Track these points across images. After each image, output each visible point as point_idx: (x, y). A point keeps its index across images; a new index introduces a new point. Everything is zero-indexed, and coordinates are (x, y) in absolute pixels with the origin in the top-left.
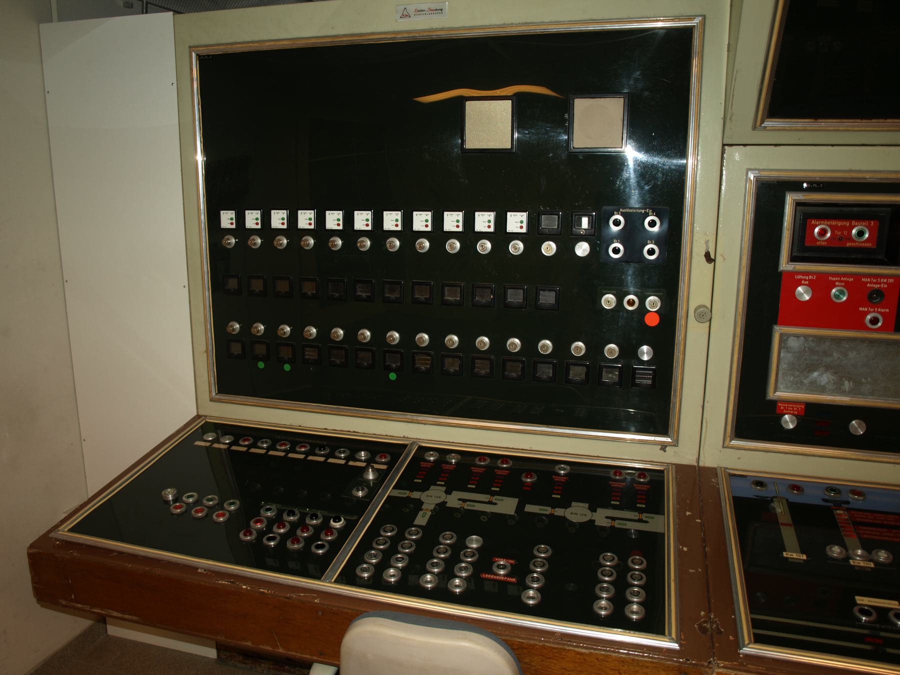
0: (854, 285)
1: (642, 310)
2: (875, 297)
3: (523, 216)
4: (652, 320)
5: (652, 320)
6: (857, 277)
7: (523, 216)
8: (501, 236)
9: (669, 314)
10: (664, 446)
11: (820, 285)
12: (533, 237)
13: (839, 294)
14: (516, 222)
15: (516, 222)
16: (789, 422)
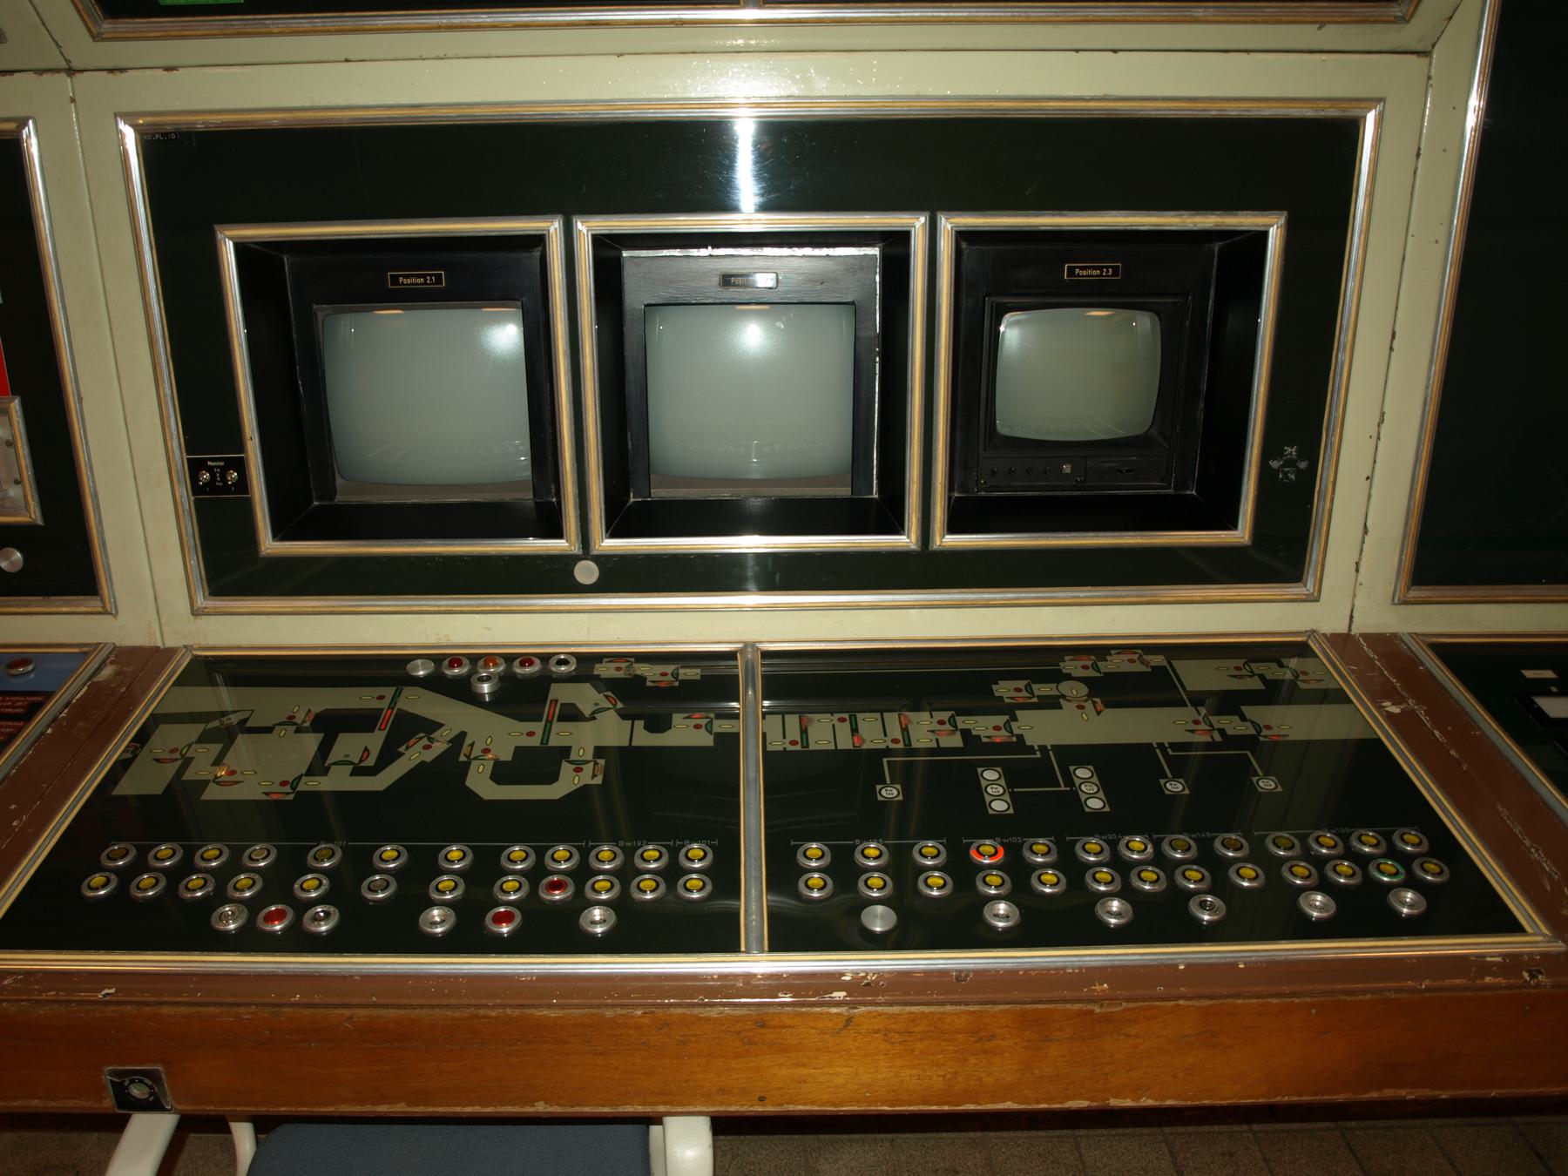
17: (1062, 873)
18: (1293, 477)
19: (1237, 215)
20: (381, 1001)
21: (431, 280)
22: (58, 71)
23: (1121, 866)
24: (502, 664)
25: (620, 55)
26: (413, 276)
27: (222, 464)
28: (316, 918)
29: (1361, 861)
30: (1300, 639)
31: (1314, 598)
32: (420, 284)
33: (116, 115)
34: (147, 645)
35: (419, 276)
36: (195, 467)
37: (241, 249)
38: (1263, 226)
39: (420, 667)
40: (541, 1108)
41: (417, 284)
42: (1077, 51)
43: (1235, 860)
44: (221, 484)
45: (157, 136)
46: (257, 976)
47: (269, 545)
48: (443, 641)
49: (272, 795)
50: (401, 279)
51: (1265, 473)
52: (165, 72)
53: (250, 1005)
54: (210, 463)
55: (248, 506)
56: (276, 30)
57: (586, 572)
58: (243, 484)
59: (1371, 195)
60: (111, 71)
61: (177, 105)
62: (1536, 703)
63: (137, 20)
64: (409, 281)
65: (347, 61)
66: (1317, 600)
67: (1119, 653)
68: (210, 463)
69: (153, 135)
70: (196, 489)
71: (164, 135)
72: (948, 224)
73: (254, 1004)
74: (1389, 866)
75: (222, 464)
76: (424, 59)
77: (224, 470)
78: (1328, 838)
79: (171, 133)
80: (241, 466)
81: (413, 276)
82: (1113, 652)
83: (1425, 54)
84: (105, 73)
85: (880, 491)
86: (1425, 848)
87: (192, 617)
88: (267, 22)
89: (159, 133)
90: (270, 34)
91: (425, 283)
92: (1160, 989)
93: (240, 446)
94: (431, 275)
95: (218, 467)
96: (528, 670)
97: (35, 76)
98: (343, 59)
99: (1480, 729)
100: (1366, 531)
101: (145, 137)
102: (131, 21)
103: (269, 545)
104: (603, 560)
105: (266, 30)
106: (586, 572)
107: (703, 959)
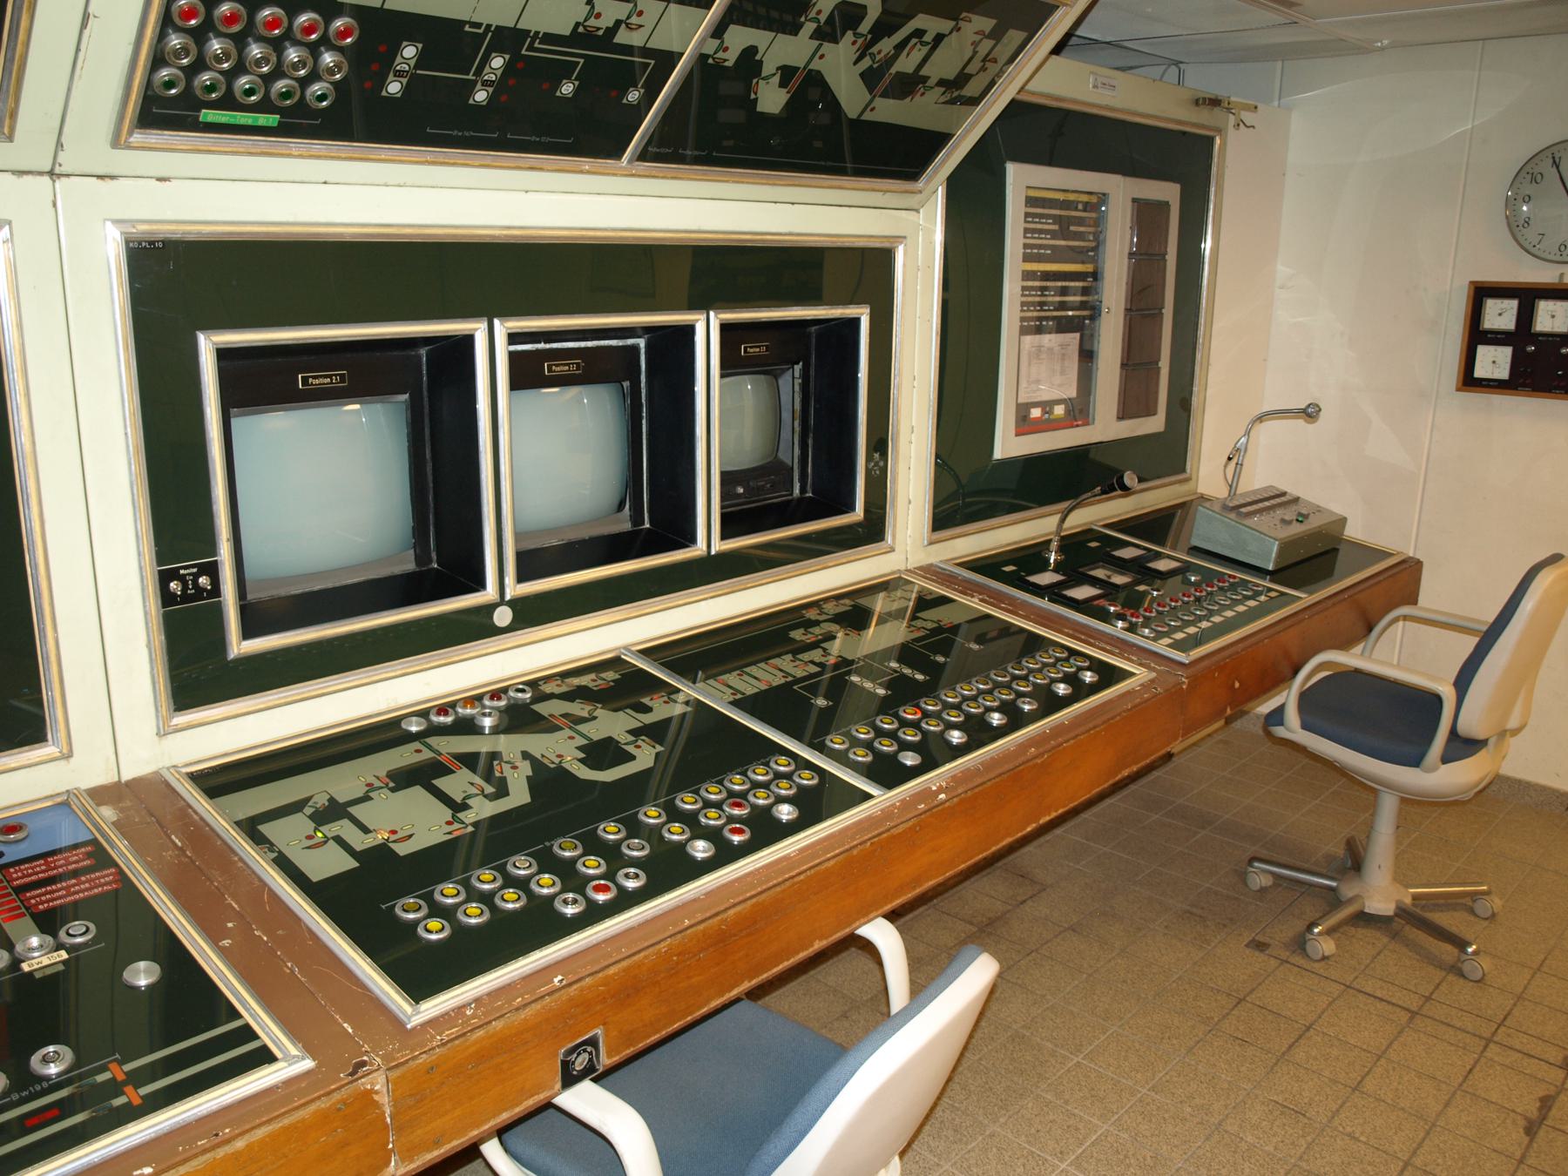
17: (484, 904)
18: (878, 472)
19: (849, 308)
20: (737, 900)
21: (336, 379)
22: (41, 173)
23: (690, 820)
24: (451, 715)
25: (527, 192)
26: (321, 376)
27: (195, 570)
28: (627, 876)
29: (487, 899)
30: (896, 576)
31: (892, 550)
32: (327, 384)
33: (105, 220)
34: (110, 781)
35: (326, 376)
36: (165, 578)
37: (223, 354)
38: (693, 320)
39: (414, 724)
40: (818, 945)
41: (324, 384)
42: (793, 204)
43: (533, 876)
44: (193, 591)
45: (144, 244)
46: (643, 924)
47: (239, 647)
48: (393, 705)
49: (455, 833)
50: (310, 380)
51: (868, 472)
52: (158, 182)
53: (666, 939)
54: (182, 572)
55: (218, 612)
56: (296, 153)
57: (503, 616)
58: (216, 590)
59: (903, 294)
60: (100, 177)
61: (170, 215)
62: (1062, 575)
63: (166, 132)
64: (317, 381)
65: (325, 183)
66: (894, 551)
67: (545, 683)
68: (182, 572)
69: (140, 243)
70: (167, 598)
71: (151, 243)
73: (668, 937)
74: (676, 827)
75: (195, 570)
76: (387, 186)
77: (196, 576)
78: (487, 875)
79: (158, 242)
80: (212, 570)
81: (321, 376)
82: (540, 683)
83: (917, 211)
84: (95, 178)
85: (651, 523)
86: (534, 869)
87: (156, 738)
88: (291, 145)
89: (146, 242)
90: (289, 156)
91: (332, 383)
92: (687, 922)
93: (212, 548)
94: (336, 375)
95: (189, 574)
96: (442, 719)
97: (14, 177)
98: (323, 181)
99: (1019, 599)
100: (910, 502)
101: (131, 245)
102: (159, 132)
103: (239, 647)
104: (513, 604)
105: (288, 152)
106: (503, 616)
107: (543, 960)
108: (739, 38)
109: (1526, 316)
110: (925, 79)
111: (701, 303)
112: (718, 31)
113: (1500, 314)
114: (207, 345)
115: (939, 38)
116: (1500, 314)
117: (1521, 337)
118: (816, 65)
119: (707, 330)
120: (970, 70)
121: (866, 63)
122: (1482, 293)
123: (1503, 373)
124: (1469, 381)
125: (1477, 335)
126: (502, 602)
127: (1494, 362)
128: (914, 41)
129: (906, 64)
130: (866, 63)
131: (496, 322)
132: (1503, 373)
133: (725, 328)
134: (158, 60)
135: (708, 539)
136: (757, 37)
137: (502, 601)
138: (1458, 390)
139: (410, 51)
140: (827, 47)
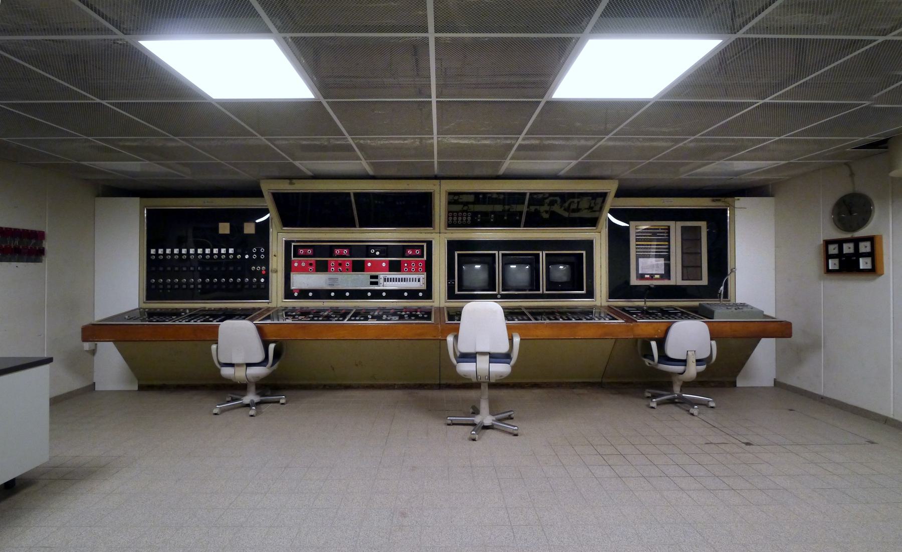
0: (306, 262)
1: (261, 270)
2: (311, 265)
3: (233, 249)
4: (264, 272)
5: (264, 272)
6: (307, 260)
7: (233, 249)
8: (227, 254)
9: (267, 270)
10: (268, 303)
11: (300, 262)
12: (235, 254)
13: (303, 264)
14: (231, 251)
15: (231, 251)
16: (296, 294)
70: (448, 284)
72: (544, 253)
80: (454, 282)
93: (454, 278)
103: (457, 292)
106: (499, 296)
108: (533, 208)
109: (841, 249)
110: (581, 209)
111: (542, 250)
112: (528, 207)
113: (834, 249)
114: (456, 253)
115: (578, 202)
116: (834, 249)
117: (840, 255)
118: (551, 209)
119: (542, 255)
120: (591, 206)
121: (563, 208)
122: (827, 243)
123: (837, 267)
124: (828, 271)
125: (828, 257)
126: (499, 294)
127: (833, 264)
128: (572, 203)
129: (574, 206)
130: (563, 208)
131: (500, 252)
132: (837, 267)
133: (547, 254)
134: (448, 220)
135: (543, 289)
136: (538, 207)
137: (499, 294)
138: (825, 273)
139: (479, 216)
140: (552, 207)
